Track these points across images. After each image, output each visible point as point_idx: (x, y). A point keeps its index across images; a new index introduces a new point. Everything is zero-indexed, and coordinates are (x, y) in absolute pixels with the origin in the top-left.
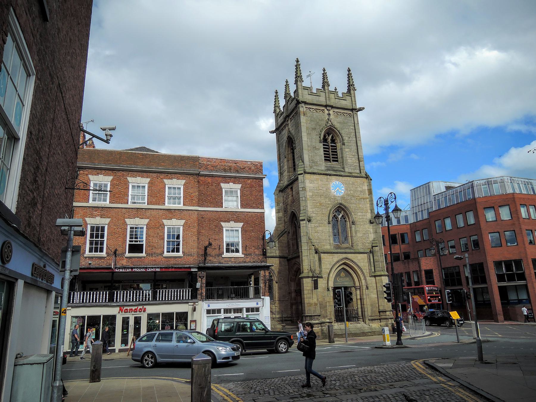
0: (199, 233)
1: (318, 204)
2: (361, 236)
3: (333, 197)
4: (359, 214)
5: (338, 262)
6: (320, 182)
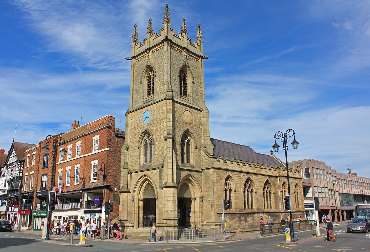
0: (84, 169)
1: (134, 135)
2: (158, 153)
3: (142, 126)
4: (158, 134)
5: (140, 179)
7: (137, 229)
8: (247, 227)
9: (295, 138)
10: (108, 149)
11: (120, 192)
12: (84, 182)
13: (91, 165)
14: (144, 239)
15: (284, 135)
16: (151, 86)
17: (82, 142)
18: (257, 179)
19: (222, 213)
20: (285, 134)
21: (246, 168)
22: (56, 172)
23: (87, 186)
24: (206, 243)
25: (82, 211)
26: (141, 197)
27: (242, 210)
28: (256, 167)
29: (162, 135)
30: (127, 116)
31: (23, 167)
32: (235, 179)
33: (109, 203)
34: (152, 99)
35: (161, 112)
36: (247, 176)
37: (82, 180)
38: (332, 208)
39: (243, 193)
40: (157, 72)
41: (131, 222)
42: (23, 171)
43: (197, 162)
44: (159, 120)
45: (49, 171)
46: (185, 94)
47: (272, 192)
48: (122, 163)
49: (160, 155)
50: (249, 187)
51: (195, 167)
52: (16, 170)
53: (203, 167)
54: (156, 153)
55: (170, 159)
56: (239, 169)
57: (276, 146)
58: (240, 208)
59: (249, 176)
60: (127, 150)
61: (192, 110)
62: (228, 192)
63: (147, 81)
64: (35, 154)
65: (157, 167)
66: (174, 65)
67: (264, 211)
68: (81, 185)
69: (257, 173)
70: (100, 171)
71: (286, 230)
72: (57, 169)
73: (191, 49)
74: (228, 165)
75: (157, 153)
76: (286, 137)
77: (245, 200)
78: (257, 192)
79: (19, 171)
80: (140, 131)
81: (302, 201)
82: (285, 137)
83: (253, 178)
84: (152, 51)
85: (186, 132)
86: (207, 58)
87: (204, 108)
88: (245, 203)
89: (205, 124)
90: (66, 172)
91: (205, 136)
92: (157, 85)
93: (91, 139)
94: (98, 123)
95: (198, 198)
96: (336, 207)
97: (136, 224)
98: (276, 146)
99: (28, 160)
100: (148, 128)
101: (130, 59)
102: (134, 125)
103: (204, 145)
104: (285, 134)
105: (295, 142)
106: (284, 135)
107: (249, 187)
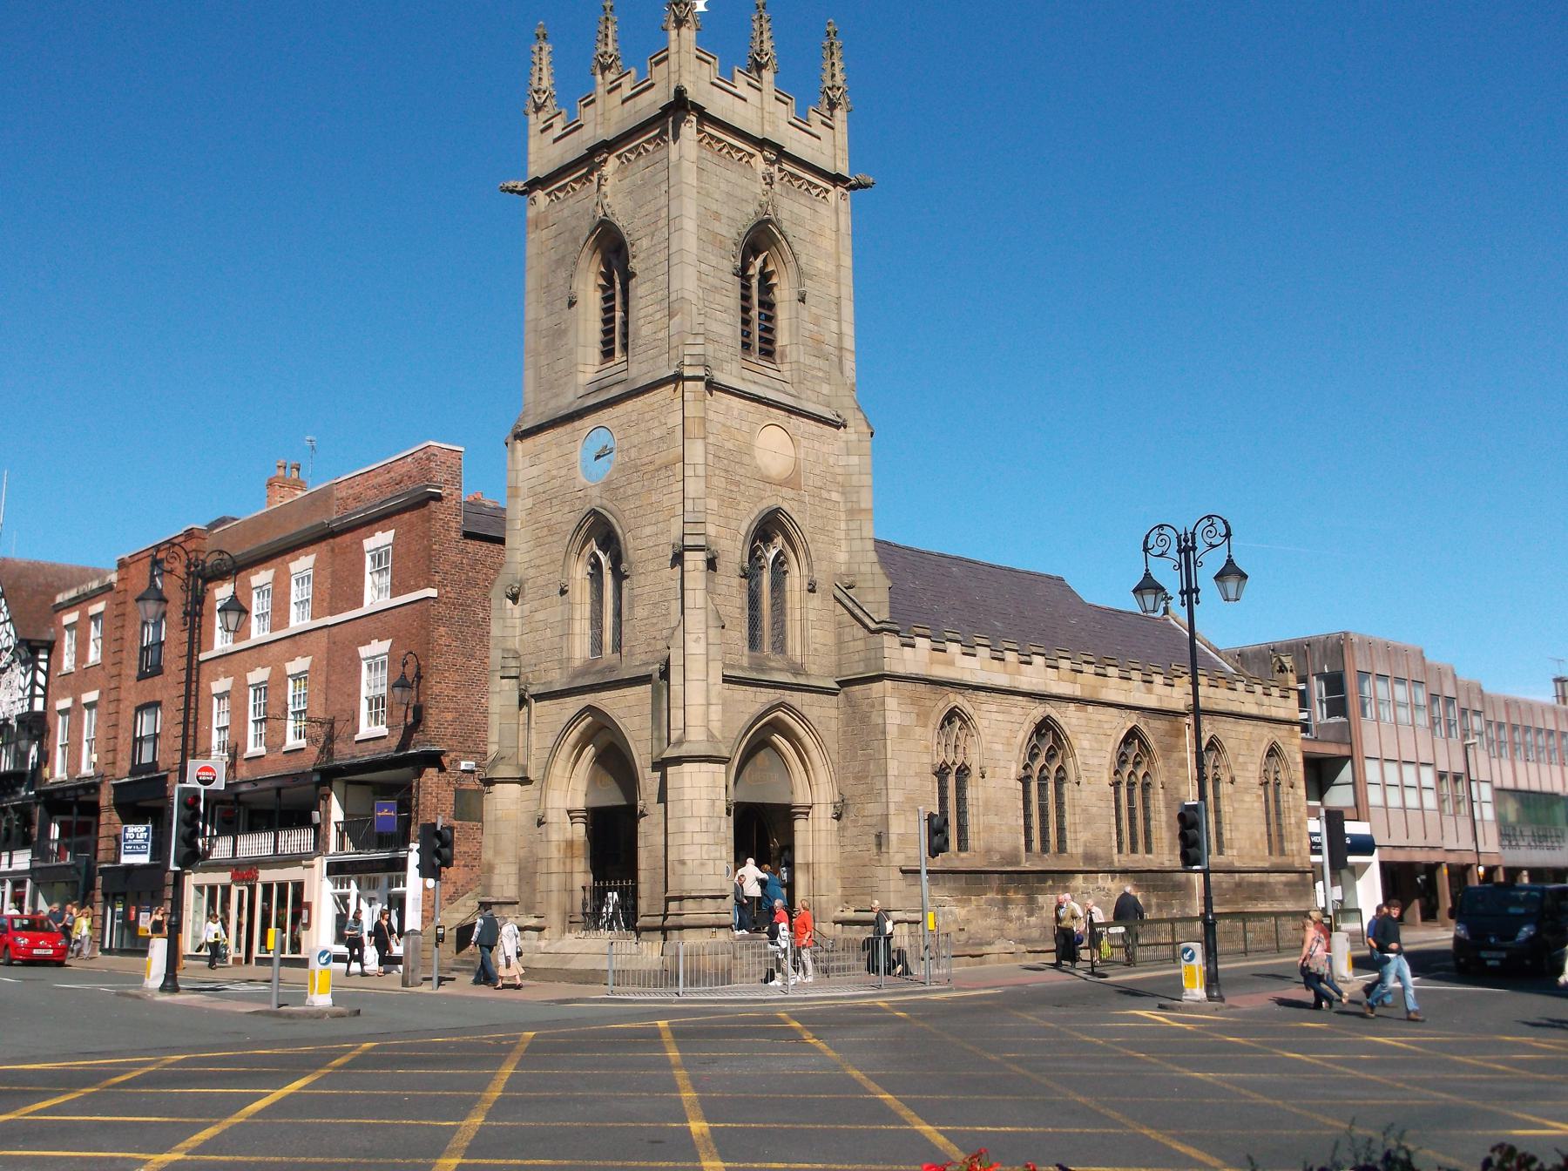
0: (328, 681)
4: (648, 531)
6: (554, 452)
7: (559, 939)
8: (1035, 933)
9: (1230, 556)
10: (432, 592)
11: (490, 782)
12: (330, 738)
13: (356, 661)
14: (586, 983)
15: (1186, 541)
16: (618, 314)
17: (316, 560)
18: (1084, 722)
19: (918, 872)
20: (1189, 536)
21: (1036, 676)
22: (202, 695)
23: (344, 753)
24: (843, 998)
25: (320, 864)
26: (580, 803)
27: (1013, 858)
28: (1081, 672)
29: (662, 533)
30: (513, 451)
31: (47, 674)
32: (985, 723)
33: (439, 828)
34: (623, 376)
35: (657, 433)
36: (1038, 711)
37: (318, 731)
38: (1453, 859)
39: (1020, 785)
40: (642, 256)
41: (534, 908)
42: (45, 689)
43: (816, 650)
44: (651, 467)
45: (168, 688)
46: (768, 351)
47: (1157, 781)
48: (495, 656)
49: (655, 621)
50: (1050, 757)
51: (807, 675)
52: (15, 684)
53: (844, 673)
54: (638, 614)
55: (697, 640)
56: (1002, 680)
57: (1148, 586)
58: (1006, 847)
59: (1051, 710)
60: (514, 598)
61: (795, 420)
62: (951, 781)
63: (599, 294)
64: (101, 613)
65: (642, 672)
66: (717, 224)
67: (1117, 865)
68: (316, 750)
69: (1087, 695)
70: (397, 691)
71: (1186, 950)
72: (203, 681)
73: (796, 143)
74: (951, 663)
75: (640, 612)
76: (1194, 549)
77: (1027, 816)
78: (1082, 781)
79: (28, 692)
80: (567, 518)
81: (1300, 824)
82: (1187, 548)
83: (1069, 718)
84: (619, 157)
85: (768, 522)
86: (866, 186)
87: (849, 415)
88: (1028, 829)
89: (854, 484)
90: (248, 696)
91: (855, 534)
92: (642, 313)
93: (355, 546)
94: (388, 476)
95: (823, 806)
96: (1478, 852)
97: (554, 919)
98: (1148, 586)
99: (68, 643)
100: (605, 502)
101: (519, 189)
102: (549, 486)
103: (848, 575)
104: (1189, 536)
105: (1230, 572)
106: (1186, 541)
107: (1050, 757)
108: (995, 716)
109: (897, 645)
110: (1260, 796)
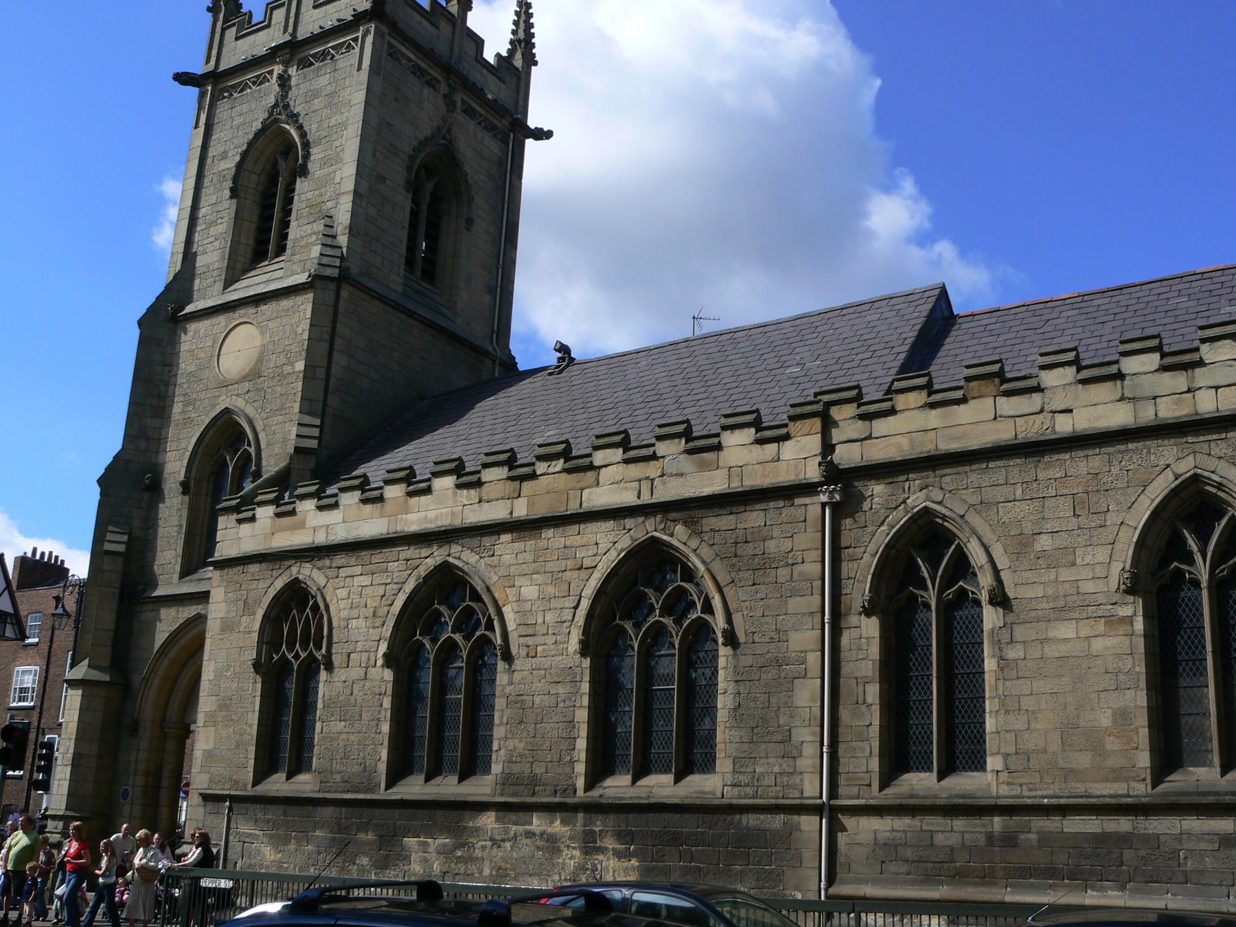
36: (433, 557)
69: (541, 511)
108: (358, 581)
109: (234, 524)
110: (1130, 620)
